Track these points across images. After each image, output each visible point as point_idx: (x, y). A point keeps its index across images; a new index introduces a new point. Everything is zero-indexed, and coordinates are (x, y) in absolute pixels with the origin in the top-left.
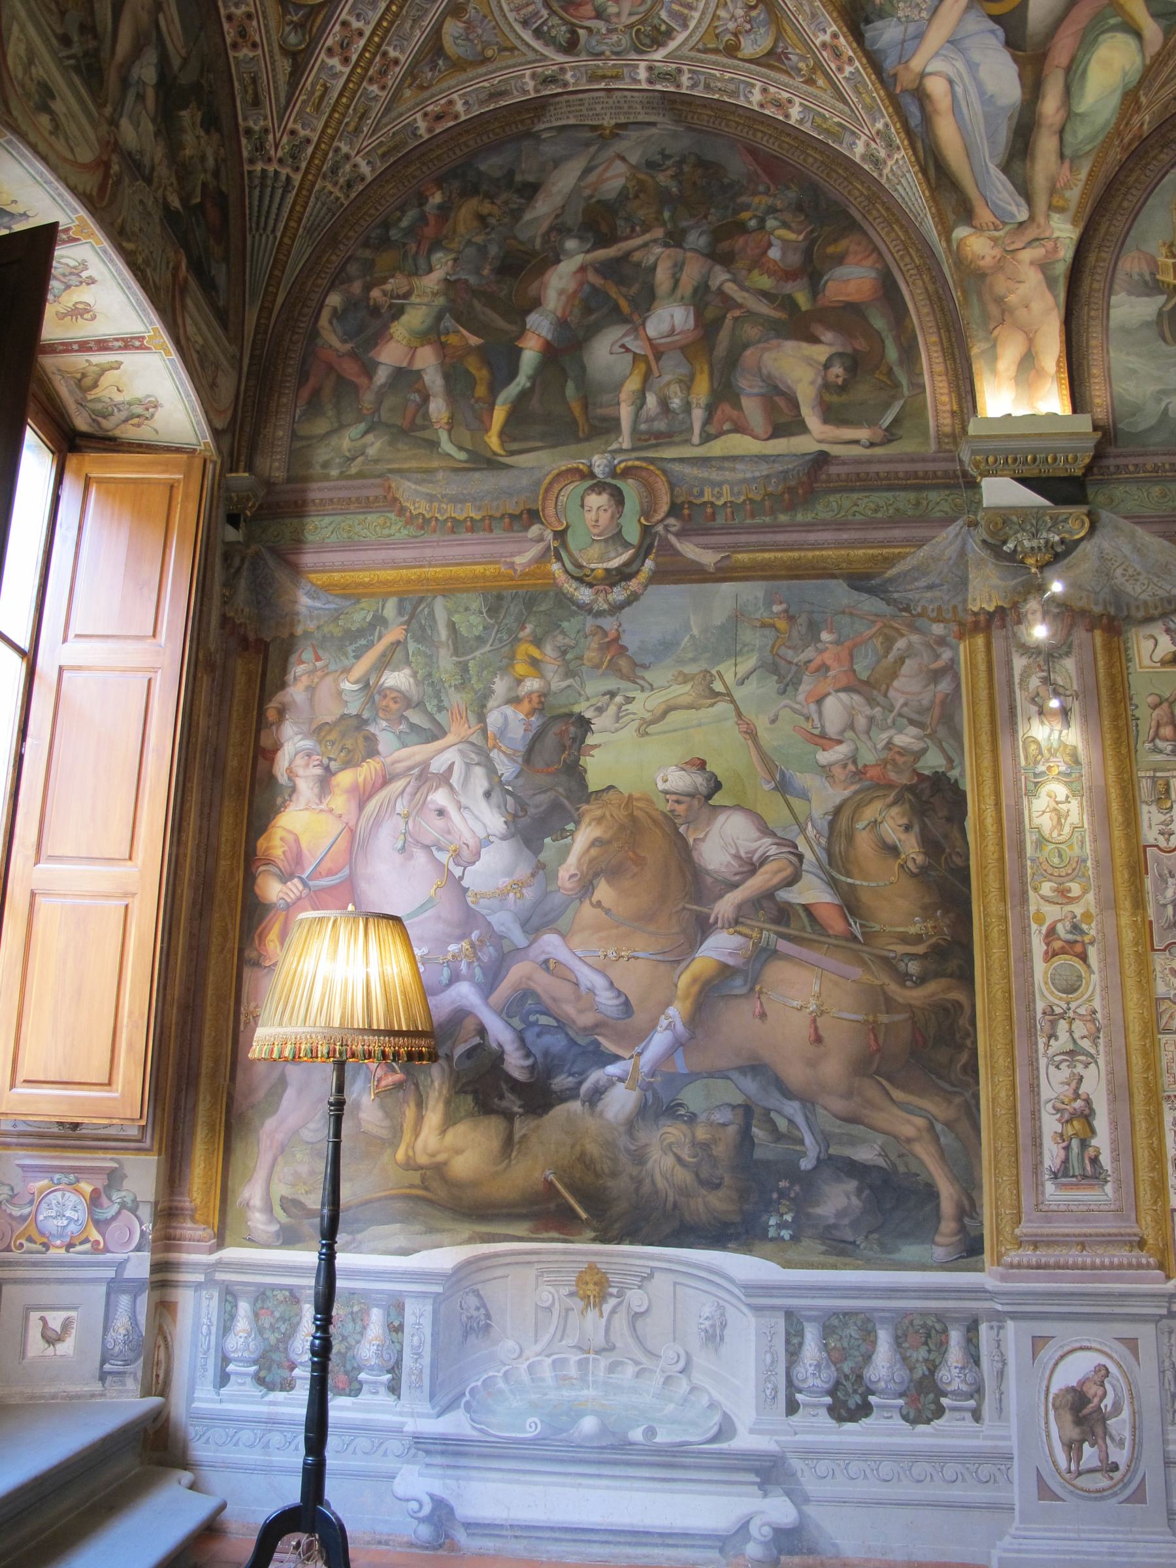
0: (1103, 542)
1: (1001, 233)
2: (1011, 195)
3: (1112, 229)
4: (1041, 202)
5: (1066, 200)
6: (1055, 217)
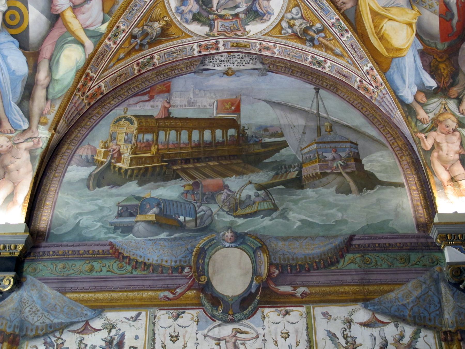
0: (24, 293)
1: (14, 135)
2: (21, 116)
3: (79, 135)
4: (35, 121)
5: (48, 120)
6: (41, 127)
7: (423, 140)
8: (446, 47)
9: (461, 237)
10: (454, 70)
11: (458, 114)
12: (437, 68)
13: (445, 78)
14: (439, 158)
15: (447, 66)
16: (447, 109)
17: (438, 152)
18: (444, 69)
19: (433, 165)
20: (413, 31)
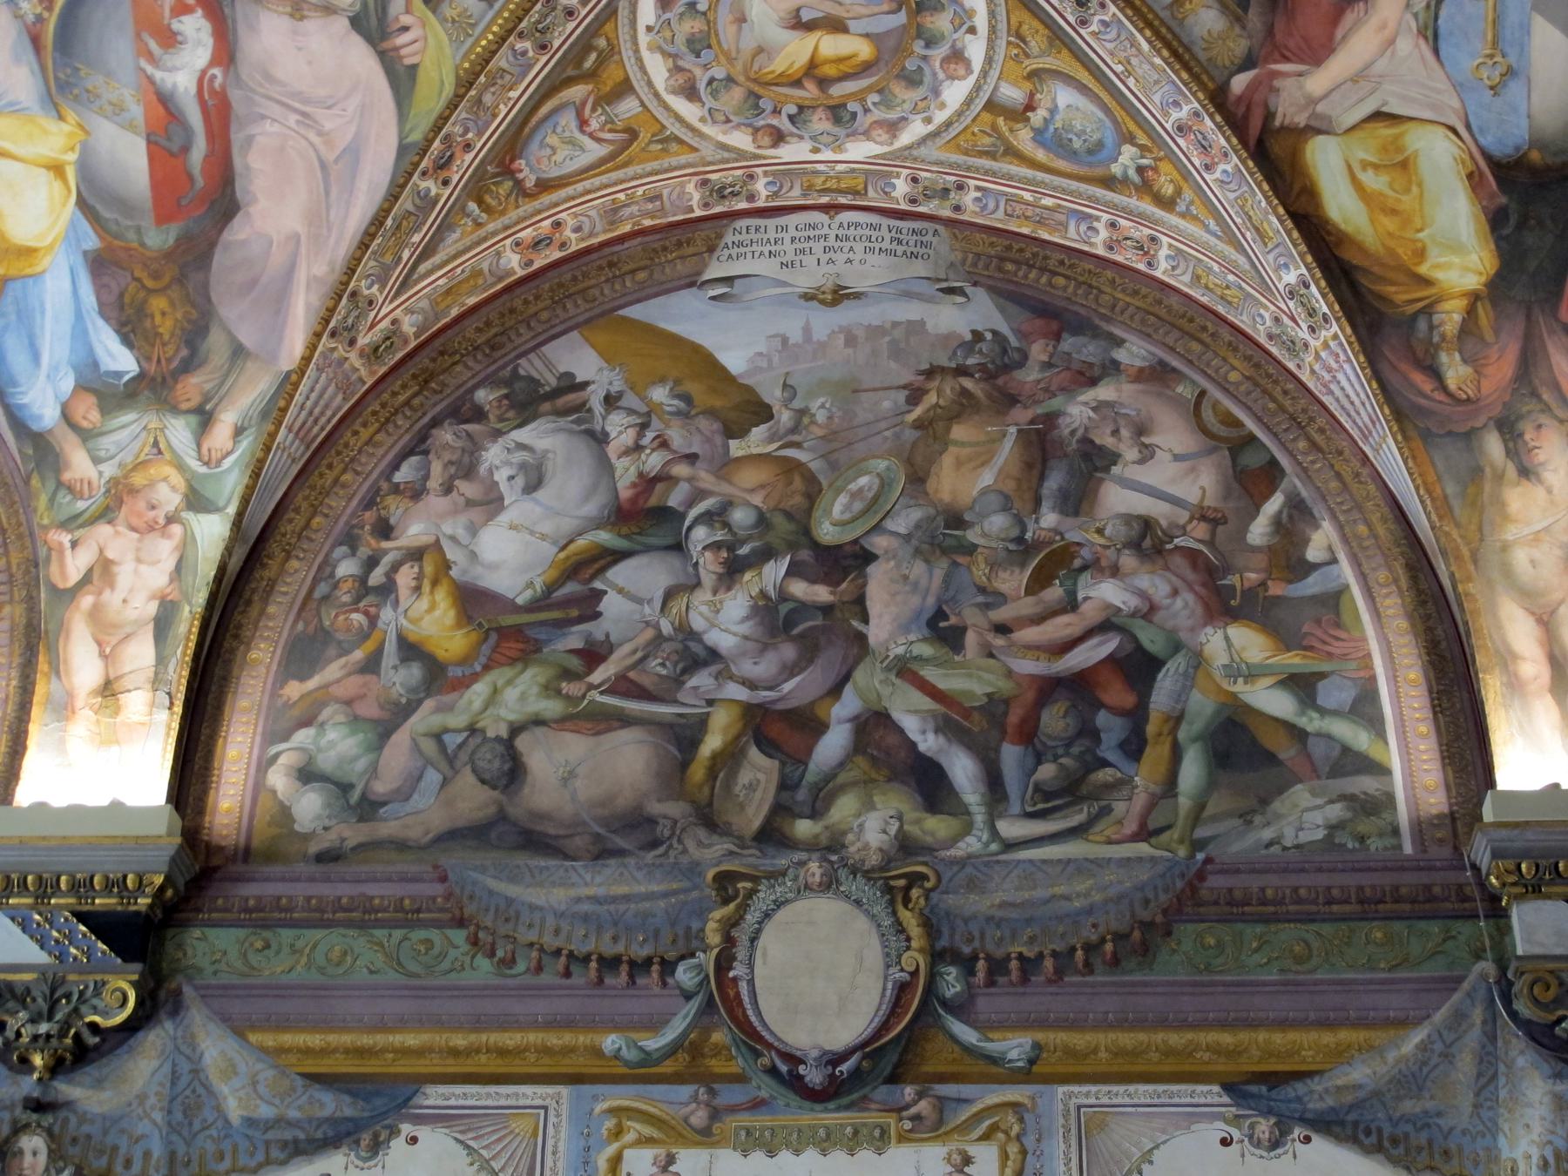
7: (61, 552)
8: (171, 241)
9: (34, 884)
10: (195, 315)
11: (194, 464)
12: (141, 311)
13: (164, 345)
14: (95, 615)
15: (172, 304)
16: (162, 446)
17: (100, 593)
18: (164, 313)
19: (67, 638)
20: (69, 191)
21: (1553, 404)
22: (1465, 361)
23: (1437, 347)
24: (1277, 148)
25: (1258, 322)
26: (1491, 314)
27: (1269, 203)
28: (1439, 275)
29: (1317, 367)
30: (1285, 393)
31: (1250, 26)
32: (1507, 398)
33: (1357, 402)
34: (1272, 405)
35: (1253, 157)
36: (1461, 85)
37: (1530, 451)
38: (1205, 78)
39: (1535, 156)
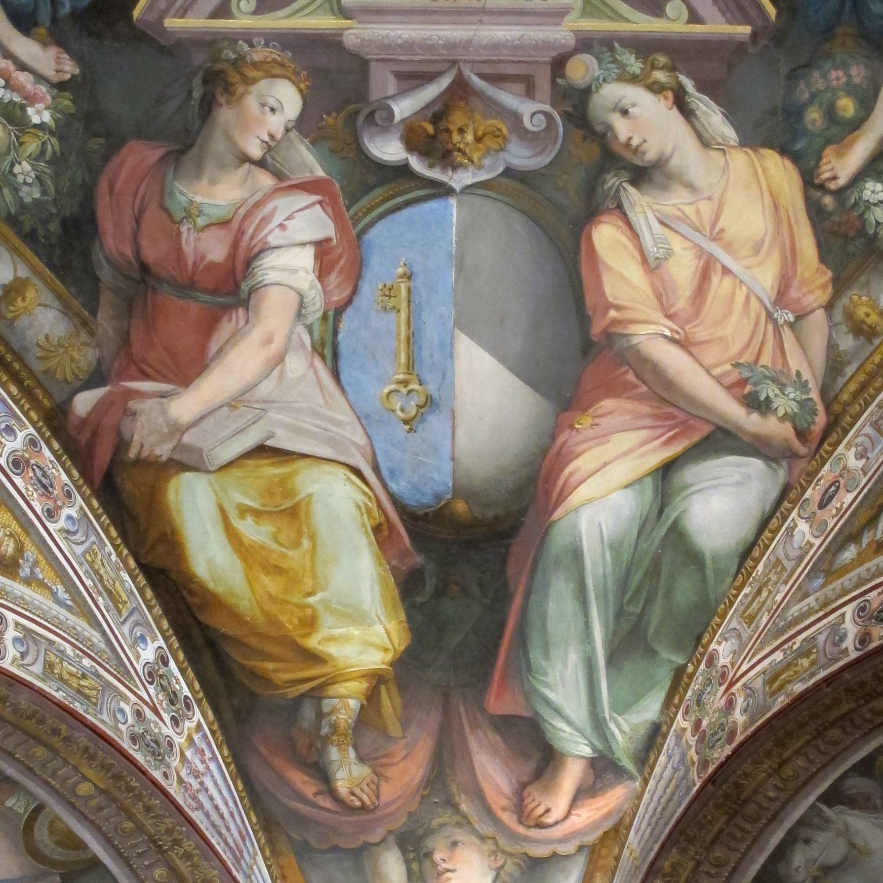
21: (474, 817)
22: (361, 759)
23: (326, 740)
24: (128, 485)
25: (117, 718)
26: (398, 700)
27: (119, 555)
28: (332, 650)
29: (183, 773)
30: (148, 809)
31: (100, 331)
32: (414, 806)
33: (227, 815)
34: (128, 825)
35: (97, 493)
36: (367, 416)
37: (439, 874)
38: (39, 392)
39: (460, 507)
